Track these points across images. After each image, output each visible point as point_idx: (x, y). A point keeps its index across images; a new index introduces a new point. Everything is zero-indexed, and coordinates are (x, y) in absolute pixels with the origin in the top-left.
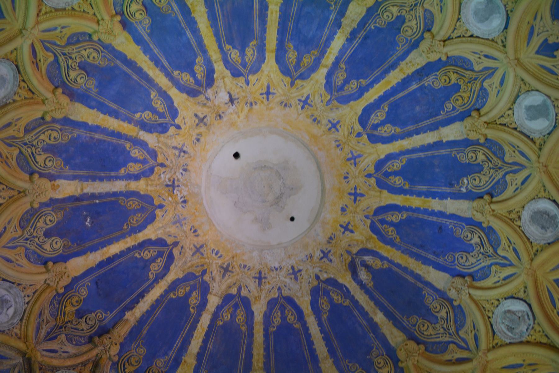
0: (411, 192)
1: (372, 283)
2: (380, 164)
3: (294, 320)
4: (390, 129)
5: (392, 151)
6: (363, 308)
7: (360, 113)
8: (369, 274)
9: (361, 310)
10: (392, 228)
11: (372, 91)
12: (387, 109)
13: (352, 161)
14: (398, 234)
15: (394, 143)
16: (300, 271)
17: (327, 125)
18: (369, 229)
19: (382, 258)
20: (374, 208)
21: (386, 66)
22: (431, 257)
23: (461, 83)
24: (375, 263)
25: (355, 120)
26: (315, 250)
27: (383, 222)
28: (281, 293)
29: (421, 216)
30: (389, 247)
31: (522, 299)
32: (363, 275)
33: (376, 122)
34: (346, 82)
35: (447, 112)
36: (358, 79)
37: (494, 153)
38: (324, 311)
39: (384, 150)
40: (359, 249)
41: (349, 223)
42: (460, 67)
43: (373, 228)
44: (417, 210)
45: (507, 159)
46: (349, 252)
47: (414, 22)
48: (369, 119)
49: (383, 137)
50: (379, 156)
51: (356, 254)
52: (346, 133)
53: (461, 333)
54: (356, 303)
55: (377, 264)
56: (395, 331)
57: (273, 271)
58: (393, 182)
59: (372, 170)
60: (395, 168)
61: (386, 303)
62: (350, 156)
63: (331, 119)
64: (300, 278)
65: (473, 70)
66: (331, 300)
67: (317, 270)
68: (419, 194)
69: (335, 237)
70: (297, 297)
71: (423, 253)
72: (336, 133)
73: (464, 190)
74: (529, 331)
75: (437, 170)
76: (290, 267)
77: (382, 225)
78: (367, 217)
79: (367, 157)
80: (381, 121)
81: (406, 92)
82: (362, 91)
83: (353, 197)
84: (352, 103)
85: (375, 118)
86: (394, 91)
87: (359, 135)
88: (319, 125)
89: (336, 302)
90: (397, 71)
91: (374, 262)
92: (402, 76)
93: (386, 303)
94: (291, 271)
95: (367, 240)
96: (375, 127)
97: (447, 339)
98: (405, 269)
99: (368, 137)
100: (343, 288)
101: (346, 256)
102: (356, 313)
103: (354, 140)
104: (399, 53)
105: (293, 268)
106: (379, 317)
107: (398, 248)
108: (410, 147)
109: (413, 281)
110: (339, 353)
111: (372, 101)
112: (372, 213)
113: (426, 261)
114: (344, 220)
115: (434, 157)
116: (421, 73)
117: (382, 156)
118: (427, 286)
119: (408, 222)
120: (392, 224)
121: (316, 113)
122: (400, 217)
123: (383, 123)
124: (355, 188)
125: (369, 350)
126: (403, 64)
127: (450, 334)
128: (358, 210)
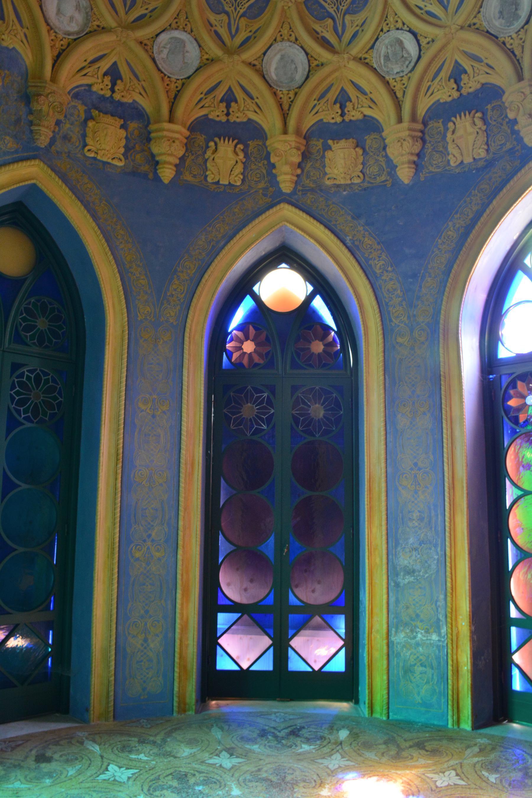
31: (419, 45)
53: (348, 17)
74: (398, 76)
97: (331, 11)
127: (338, 8)
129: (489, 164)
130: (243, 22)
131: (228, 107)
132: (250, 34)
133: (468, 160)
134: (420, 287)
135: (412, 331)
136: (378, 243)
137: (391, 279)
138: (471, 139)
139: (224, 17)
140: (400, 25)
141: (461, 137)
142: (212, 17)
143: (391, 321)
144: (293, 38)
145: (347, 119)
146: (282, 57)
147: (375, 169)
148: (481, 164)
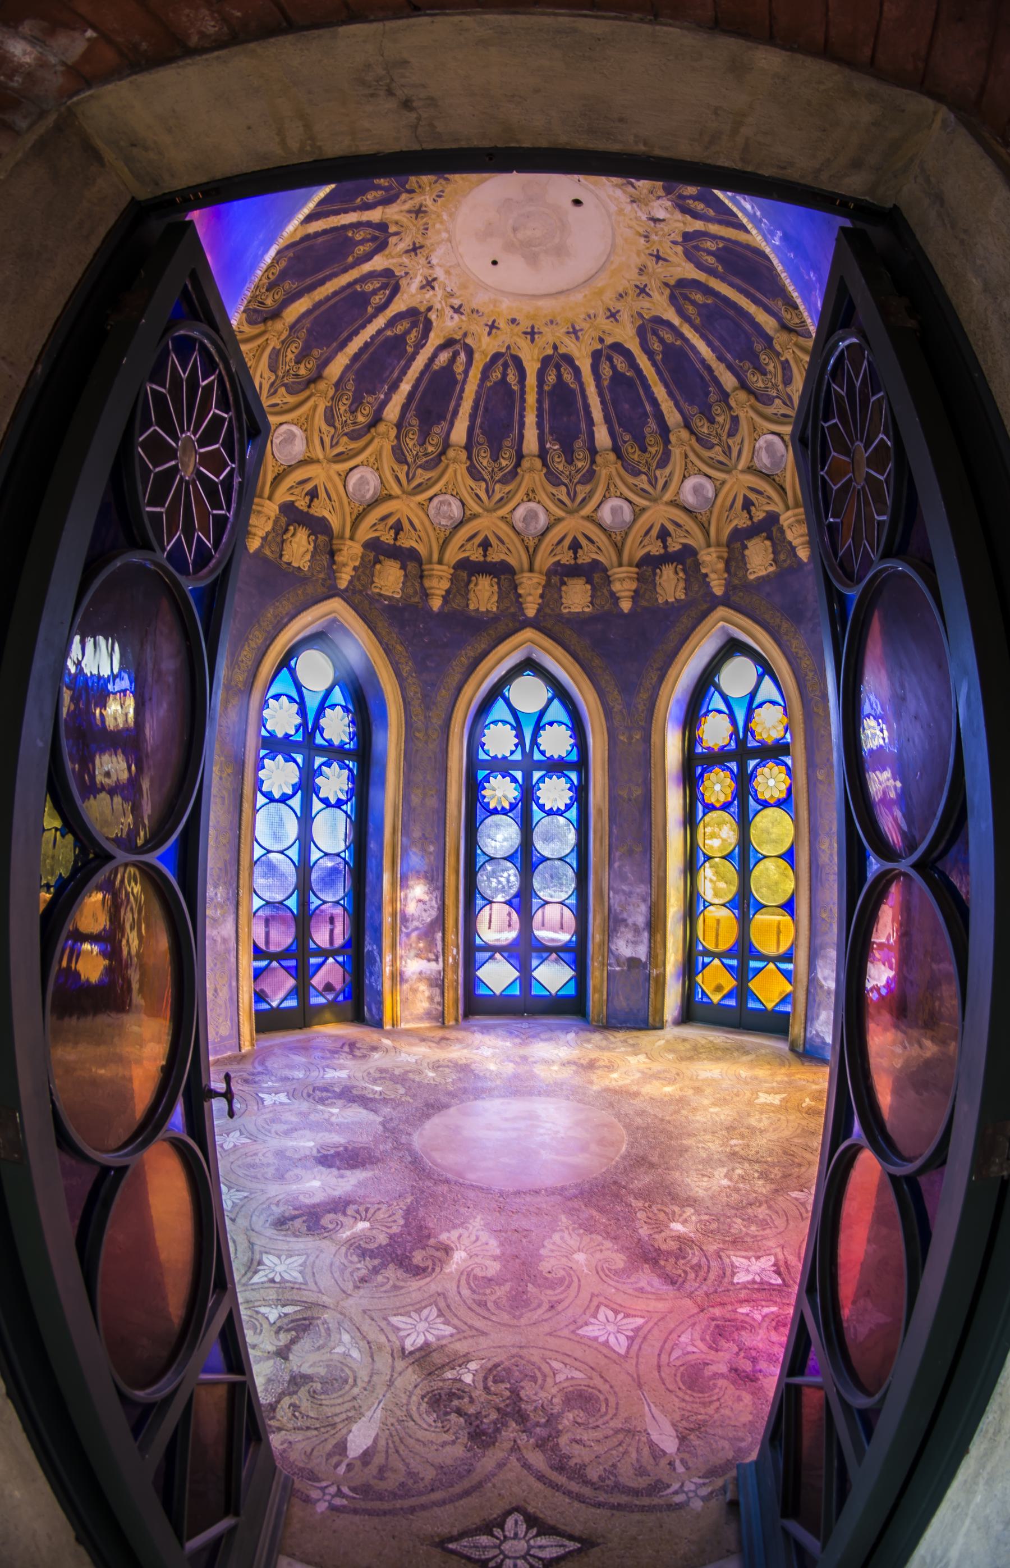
2: (568, 359)
5: (583, 374)
6: (409, 368)
7: (627, 346)
9: (407, 366)
10: (500, 376)
11: (648, 364)
13: (571, 330)
14: (495, 383)
18: (494, 351)
19: (466, 372)
20: (520, 355)
22: (479, 421)
25: (619, 339)
27: (506, 366)
29: (517, 404)
30: (479, 376)
32: (444, 357)
34: (661, 340)
36: (663, 353)
37: (584, 475)
41: (498, 328)
43: (496, 357)
44: (523, 400)
45: (579, 488)
46: (465, 335)
47: (706, 431)
50: (578, 359)
52: (605, 327)
54: (413, 358)
55: (459, 368)
59: (562, 350)
61: (421, 388)
68: (539, 401)
71: (480, 412)
73: (548, 446)
75: (565, 419)
78: (508, 347)
81: (643, 397)
82: (650, 354)
83: (529, 330)
84: (637, 340)
86: (647, 387)
87: (601, 340)
90: (666, 396)
92: (660, 400)
93: (421, 388)
94: (430, 279)
95: (483, 352)
96: (610, 359)
98: (460, 398)
102: (403, 363)
103: (596, 334)
104: (681, 402)
106: (405, 387)
107: (481, 386)
108: (588, 393)
109: (451, 409)
111: (638, 361)
112: (513, 352)
113: (473, 417)
115: (578, 416)
117: (577, 363)
119: (511, 393)
120: (504, 375)
123: (613, 367)
124: (540, 333)
125: (372, 392)
126: (671, 403)
128: (515, 337)
129: (495, 619)
130: (345, 439)
131: (311, 501)
133: (483, 609)
135: (427, 728)
138: (487, 594)
139: (332, 430)
140: (455, 493)
141: (480, 590)
142: (324, 427)
144: (375, 467)
145: (398, 543)
146: (362, 477)
147: (411, 591)
148: (491, 615)
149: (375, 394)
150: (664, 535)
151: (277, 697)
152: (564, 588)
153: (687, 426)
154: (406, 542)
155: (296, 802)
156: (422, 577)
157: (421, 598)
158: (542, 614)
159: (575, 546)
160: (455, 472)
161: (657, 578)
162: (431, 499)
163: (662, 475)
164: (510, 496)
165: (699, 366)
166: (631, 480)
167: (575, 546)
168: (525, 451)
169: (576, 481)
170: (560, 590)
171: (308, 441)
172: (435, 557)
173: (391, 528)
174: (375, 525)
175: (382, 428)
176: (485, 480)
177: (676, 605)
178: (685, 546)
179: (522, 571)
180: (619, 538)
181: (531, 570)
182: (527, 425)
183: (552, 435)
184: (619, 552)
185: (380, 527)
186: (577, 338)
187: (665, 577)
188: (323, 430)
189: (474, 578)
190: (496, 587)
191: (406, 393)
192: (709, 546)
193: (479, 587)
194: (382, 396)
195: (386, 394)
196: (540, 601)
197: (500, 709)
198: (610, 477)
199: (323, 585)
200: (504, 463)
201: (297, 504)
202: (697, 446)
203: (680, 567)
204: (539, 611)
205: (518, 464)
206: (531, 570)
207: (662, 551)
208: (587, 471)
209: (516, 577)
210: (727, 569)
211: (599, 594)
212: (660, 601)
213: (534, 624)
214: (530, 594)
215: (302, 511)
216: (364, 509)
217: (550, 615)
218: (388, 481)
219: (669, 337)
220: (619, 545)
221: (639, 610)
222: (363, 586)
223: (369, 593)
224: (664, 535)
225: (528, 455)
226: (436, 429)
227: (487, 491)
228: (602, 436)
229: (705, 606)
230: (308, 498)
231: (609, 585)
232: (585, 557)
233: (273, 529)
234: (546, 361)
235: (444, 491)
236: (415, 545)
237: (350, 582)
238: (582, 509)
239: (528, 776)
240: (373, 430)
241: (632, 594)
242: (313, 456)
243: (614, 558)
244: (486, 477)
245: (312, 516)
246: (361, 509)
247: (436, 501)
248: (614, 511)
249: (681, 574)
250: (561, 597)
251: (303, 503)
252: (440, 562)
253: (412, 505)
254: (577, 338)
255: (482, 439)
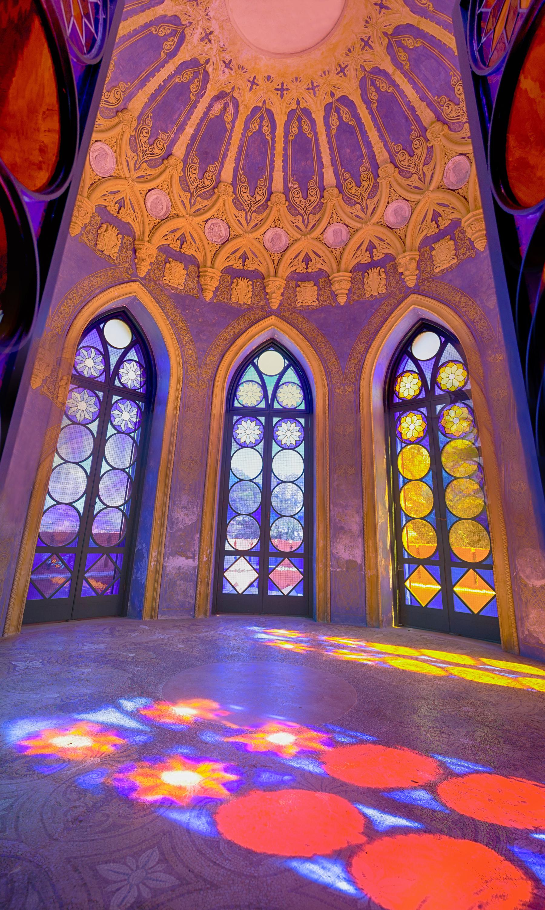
0: (286, 142)
1: (213, 117)
2: (307, 112)
3: (167, 50)
4: (335, 125)
5: (317, 126)
6: (192, 114)
8: (220, 112)
9: (190, 113)
11: (367, 112)
12: (350, 123)
13: (310, 86)
14: (254, 133)
15: (324, 128)
16: (210, 41)
17: (344, 63)
19: (233, 122)
20: (272, 109)
21: (383, 130)
22: (241, 164)
23: (361, 187)
24: (229, 116)
26: (231, 54)
27: (262, 118)
28: (186, 27)
29: (269, 151)
32: (218, 107)
33: (341, 112)
35: (343, 174)
38: (181, 77)
39: (319, 116)
40: (238, 99)
41: (258, 85)
42: (372, 189)
43: (256, 109)
44: (274, 148)
48: (345, 106)
49: (329, 117)
51: (232, 96)
54: (194, 106)
55: (228, 118)
56: (184, 148)
57: (205, 11)
58: (294, 125)
60: (304, 127)
62: (315, 84)
63: (348, 68)
64: (203, 43)
65: (368, 198)
66: (191, 82)
67: (213, 60)
68: (285, 149)
69: (244, 72)
70: (187, 45)
71: (243, 157)
72: (336, 72)
76: (212, 29)
77: (259, 118)
79: (314, 101)
80: (342, 117)
82: (367, 102)
83: (280, 87)
85: (345, 111)
86: (364, 133)
87: (332, 94)
88: (344, 55)
89: (191, 87)
91: (230, 115)
96: (338, 111)
98: (229, 144)
99: (330, 103)
100: (203, 90)
101: (230, 87)
102: (187, 108)
104: (389, 143)
105: (211, 33)
106: (189, 130)
107: (243, 135)
109: (222, 152)
110: (154, 105)
111: (359, 111)
112: (268, 107)
113: (238, 160)
114: (260, 80)
115: (312, 161)
116: (372, 157)
117: (314, 116)
118: (221, 164)
119: (265, 141)
120: (261, 126)
121: (355, 53)
122: (267, 133)
123: (340, 118)
124: (288, 89)
126: (381, 144)
128: (269, 93)
132: (145, 175)
134: (206, 359)
136: (186, 327)
137: (191, 349)
143: (187, 372)
144: (167, 192)
145: (183, 251)
146: (157, 198)
149: (167, 133)
150: (371, 248)
151: (87, 348)
152: (298, 289)
153: (393, 162)
154: (188, 250)
155: (94, 427)
156: (199, 277)
157: (198, 291)
158: (282, 307)
159: (307, 260)
160: (224, 201)
161: (365, 279)
162: (207, 221)
163: (371, 203)
164: (262, 222)
165: (405, 108)
166: (348, 209)
167: (307, 260)
168: (273, 189)
169: (309, 212)
170: (296, 291)
171: (118, 161)
172: (209, 263)
173: (178, 239)
174: (167, 235)
175: (172, 160)
176: (244, 210)
177: (378, 297)
178: (386, 254)
179: (269, 276)
180: (338, 253)
181: (275, 276)
182: (275, 170)
183: (293, 177)
184: (339, 263)
185: (170, 237)
186: (315, 94)
187: (370, 278)
188: (129, 155)
189: (235, 280)
190: (251, 287)
191: (190, 136)
192: (405, 251)
193: (239, 287)
194: (172, 135)
195: (175, 134)
196: (282, 298)
197: (250, 374)
198: (334, 208)
199: (128, 273)
200: (259, 197)
201: (108, 208)
202: (398, 177)
203: (383, 270)
204: (280, 305)
205: (269, 199)
206: (275, 276)
207: (370, 260)
208: (317, 205)
209: (265, 281)
210: (418, 267)
211: (323, 293)
212: (367, 296)
213: (277, 313)
214: (274, 293)
215: (113, 215)
216: (159, 222)
217: (288, 308)
218: (176, 204)
219: (383, 85)
220: (338, 257)
221: (351, 303)
222: (156, 277)
223: (161, 283)
224: (371, 248)
225: (275, 192)
226: (211, 168)
227: (246, 219)
228: (329, 177)
229: (401, 296)
230: (117, 206)
231: (330, 287)
232: (314, 267)
233: (90, 223)
234: (291, 114)
235: (216, 216)
236: (194, 254)
237: (148, 273)
238: (313, 231)
239: (269, 421)
240: (166, 161)
241: (347, 292)
242: (121, 174)
243: (335, 266)
244: (246, 208)
245: (120, 220)
246: (157, 221)
247: (210, 222)
248: (335, 233)
249: (383, 275)
250: (296, 296)
251: (113, 209)
252: (212, 267)
253: (193, 223)
254: (315, 94)
255: (243, 178)
